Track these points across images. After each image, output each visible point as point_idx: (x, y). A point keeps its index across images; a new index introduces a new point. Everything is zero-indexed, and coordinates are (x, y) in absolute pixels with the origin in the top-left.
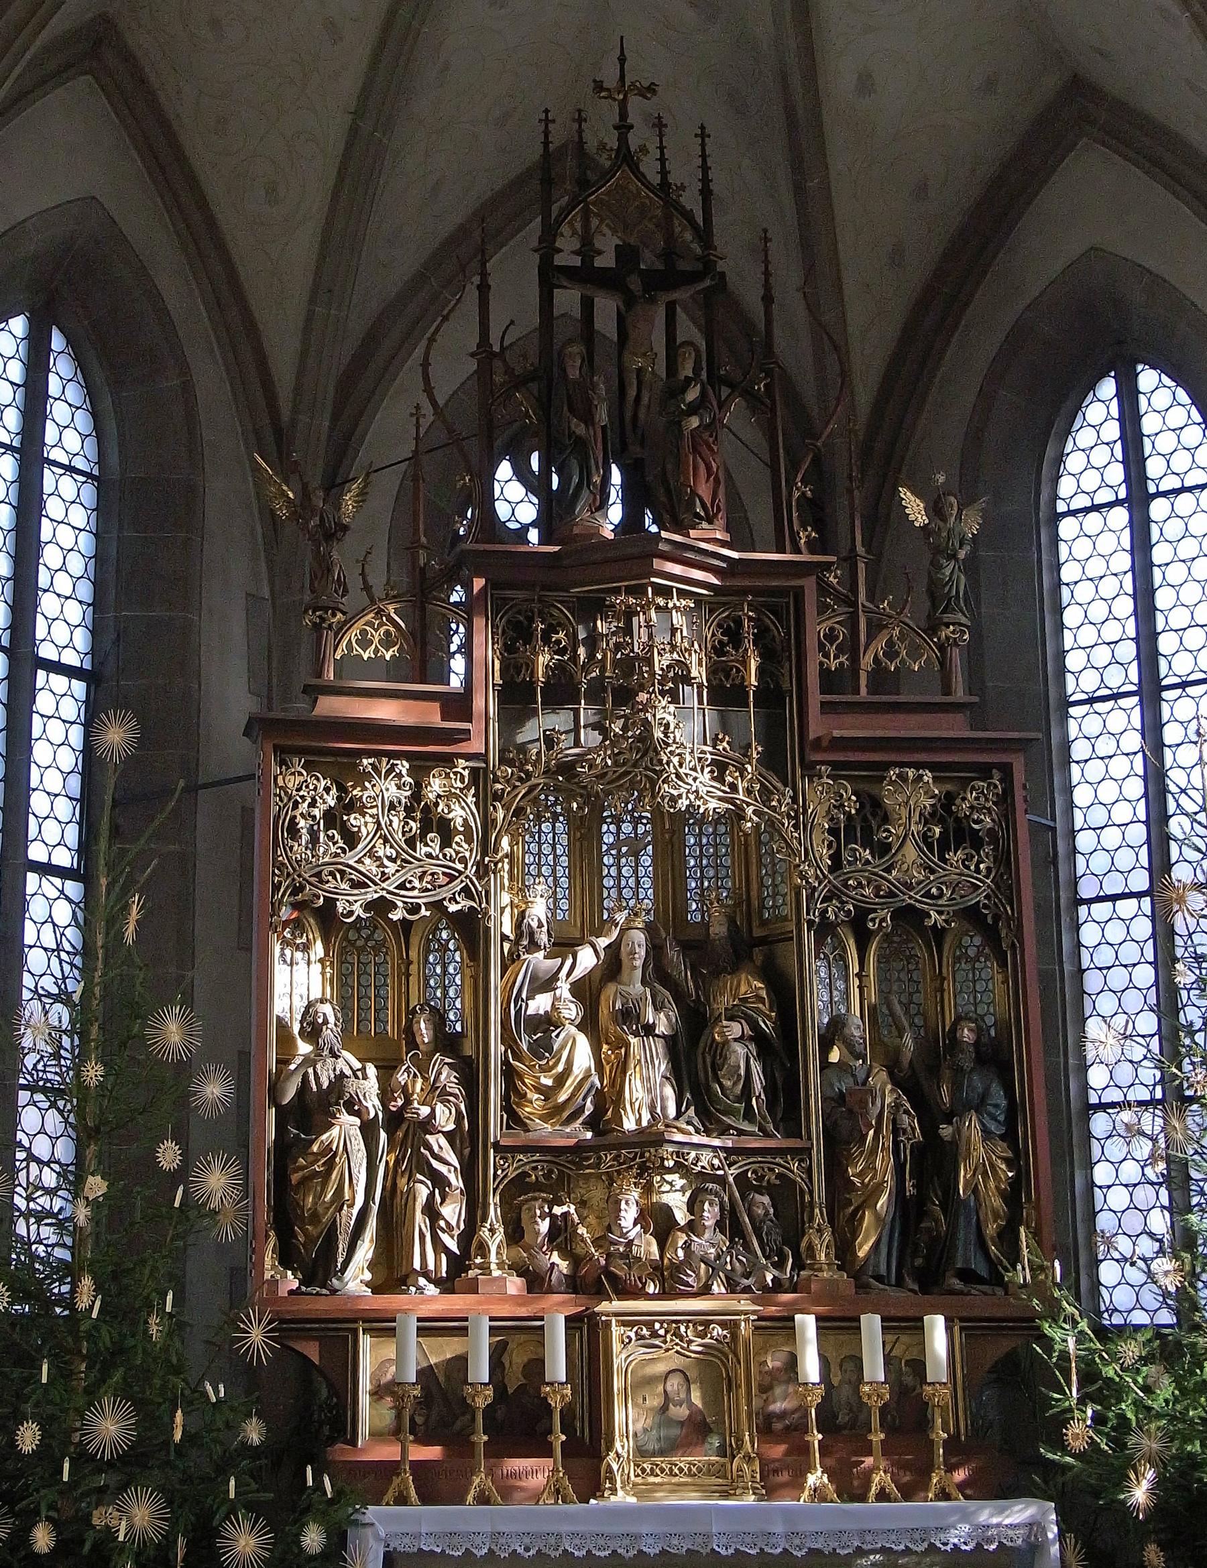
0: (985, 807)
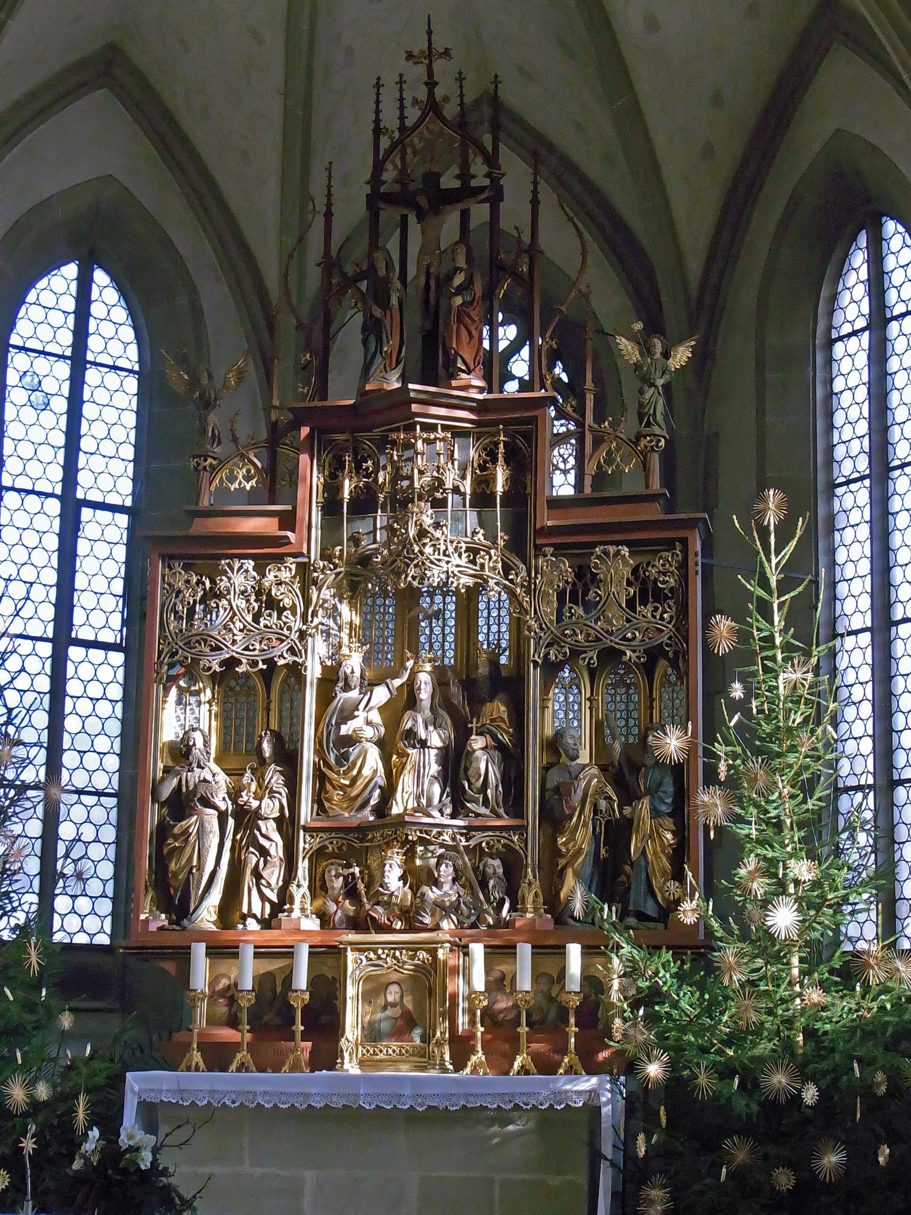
0: (669, 572)
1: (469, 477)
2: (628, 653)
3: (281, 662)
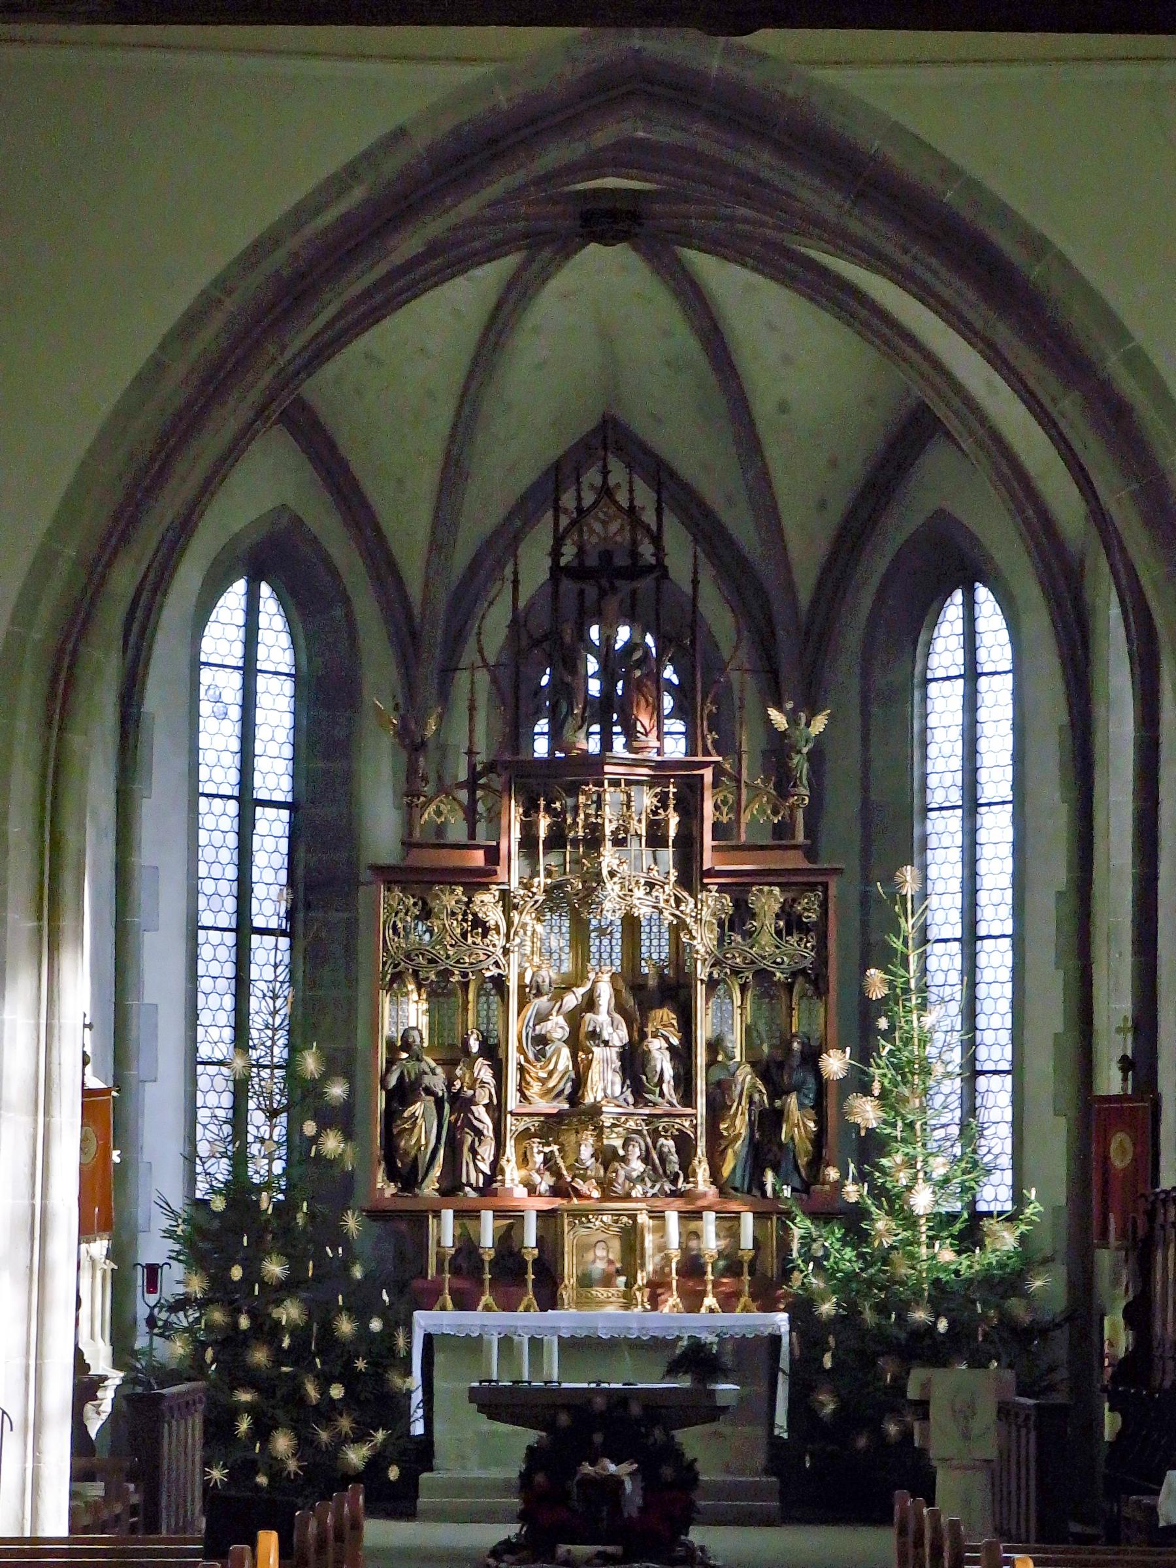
1: (644, 822)
2: (778, 974)
3: (488, 974)
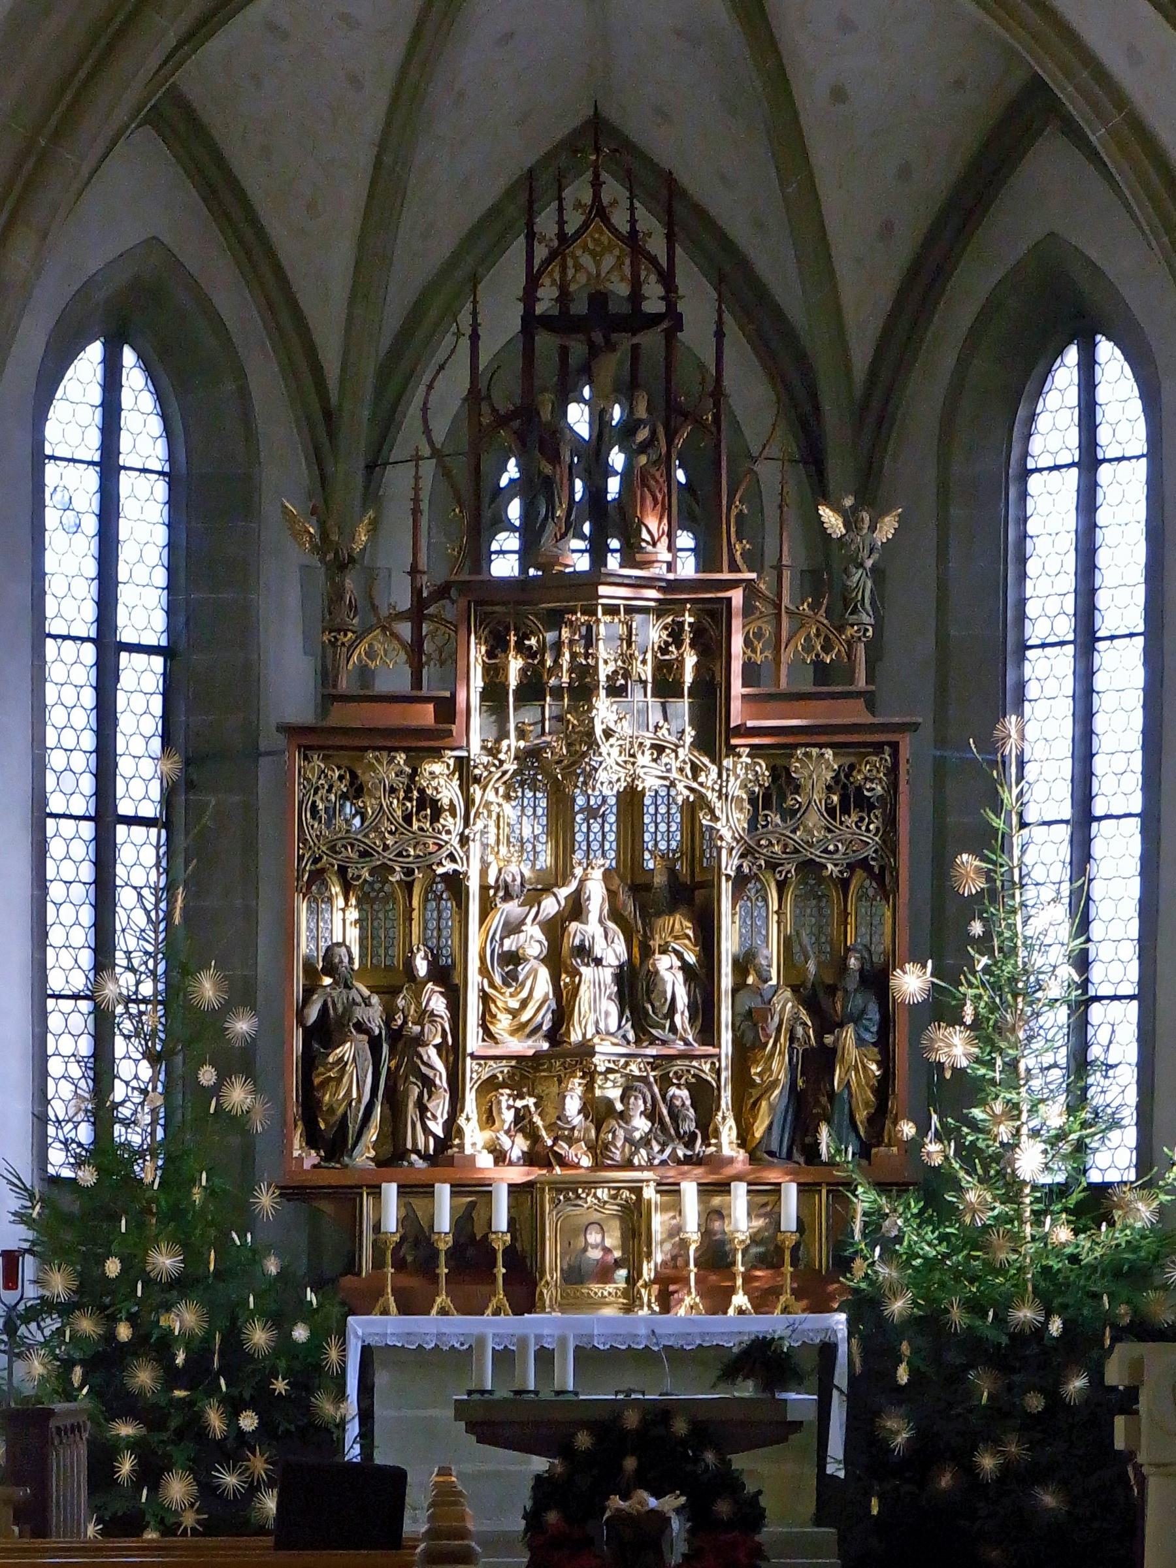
2: (830, 866)
3: (440, 870)
